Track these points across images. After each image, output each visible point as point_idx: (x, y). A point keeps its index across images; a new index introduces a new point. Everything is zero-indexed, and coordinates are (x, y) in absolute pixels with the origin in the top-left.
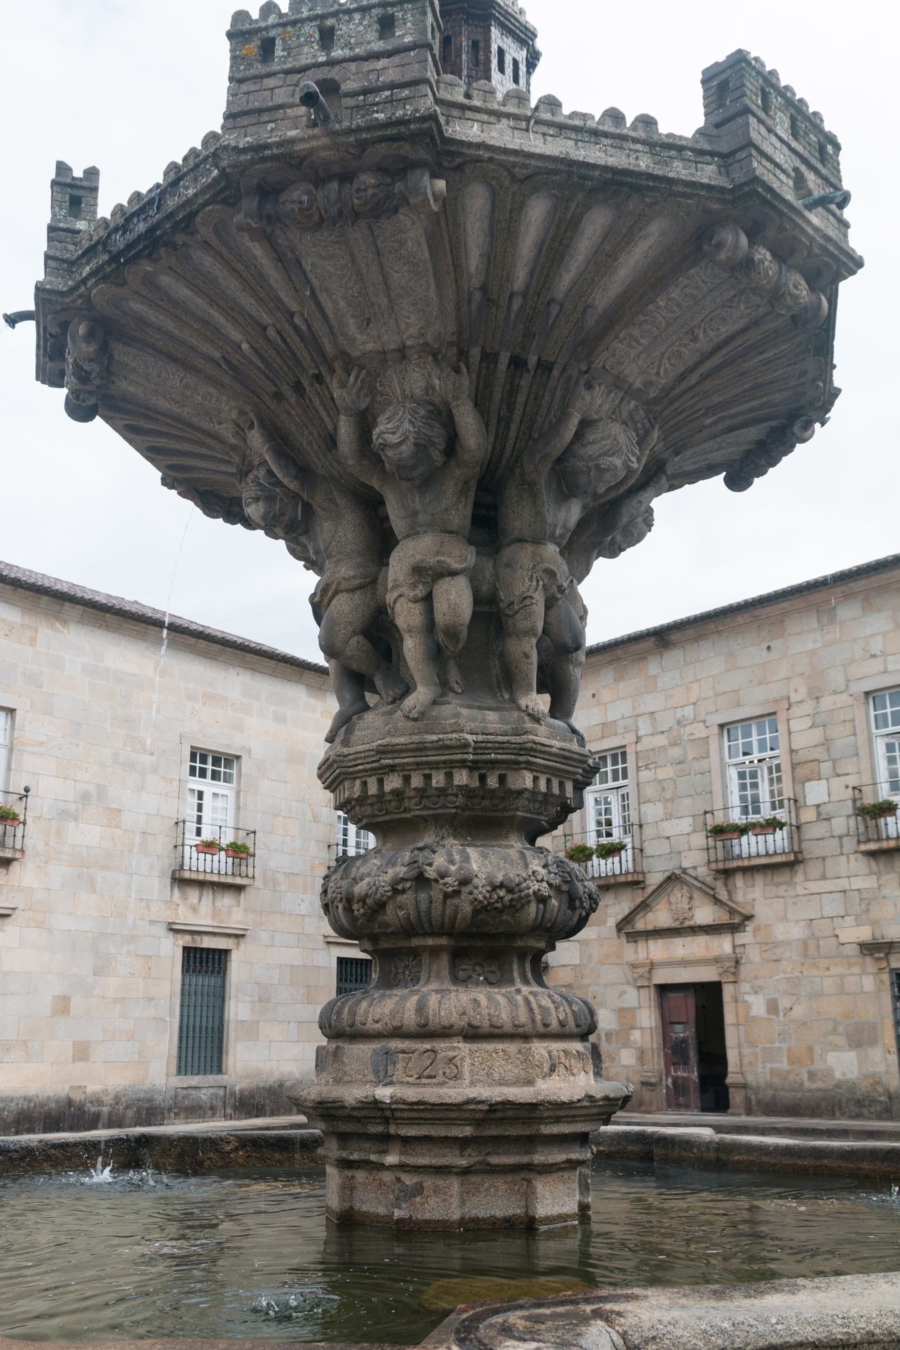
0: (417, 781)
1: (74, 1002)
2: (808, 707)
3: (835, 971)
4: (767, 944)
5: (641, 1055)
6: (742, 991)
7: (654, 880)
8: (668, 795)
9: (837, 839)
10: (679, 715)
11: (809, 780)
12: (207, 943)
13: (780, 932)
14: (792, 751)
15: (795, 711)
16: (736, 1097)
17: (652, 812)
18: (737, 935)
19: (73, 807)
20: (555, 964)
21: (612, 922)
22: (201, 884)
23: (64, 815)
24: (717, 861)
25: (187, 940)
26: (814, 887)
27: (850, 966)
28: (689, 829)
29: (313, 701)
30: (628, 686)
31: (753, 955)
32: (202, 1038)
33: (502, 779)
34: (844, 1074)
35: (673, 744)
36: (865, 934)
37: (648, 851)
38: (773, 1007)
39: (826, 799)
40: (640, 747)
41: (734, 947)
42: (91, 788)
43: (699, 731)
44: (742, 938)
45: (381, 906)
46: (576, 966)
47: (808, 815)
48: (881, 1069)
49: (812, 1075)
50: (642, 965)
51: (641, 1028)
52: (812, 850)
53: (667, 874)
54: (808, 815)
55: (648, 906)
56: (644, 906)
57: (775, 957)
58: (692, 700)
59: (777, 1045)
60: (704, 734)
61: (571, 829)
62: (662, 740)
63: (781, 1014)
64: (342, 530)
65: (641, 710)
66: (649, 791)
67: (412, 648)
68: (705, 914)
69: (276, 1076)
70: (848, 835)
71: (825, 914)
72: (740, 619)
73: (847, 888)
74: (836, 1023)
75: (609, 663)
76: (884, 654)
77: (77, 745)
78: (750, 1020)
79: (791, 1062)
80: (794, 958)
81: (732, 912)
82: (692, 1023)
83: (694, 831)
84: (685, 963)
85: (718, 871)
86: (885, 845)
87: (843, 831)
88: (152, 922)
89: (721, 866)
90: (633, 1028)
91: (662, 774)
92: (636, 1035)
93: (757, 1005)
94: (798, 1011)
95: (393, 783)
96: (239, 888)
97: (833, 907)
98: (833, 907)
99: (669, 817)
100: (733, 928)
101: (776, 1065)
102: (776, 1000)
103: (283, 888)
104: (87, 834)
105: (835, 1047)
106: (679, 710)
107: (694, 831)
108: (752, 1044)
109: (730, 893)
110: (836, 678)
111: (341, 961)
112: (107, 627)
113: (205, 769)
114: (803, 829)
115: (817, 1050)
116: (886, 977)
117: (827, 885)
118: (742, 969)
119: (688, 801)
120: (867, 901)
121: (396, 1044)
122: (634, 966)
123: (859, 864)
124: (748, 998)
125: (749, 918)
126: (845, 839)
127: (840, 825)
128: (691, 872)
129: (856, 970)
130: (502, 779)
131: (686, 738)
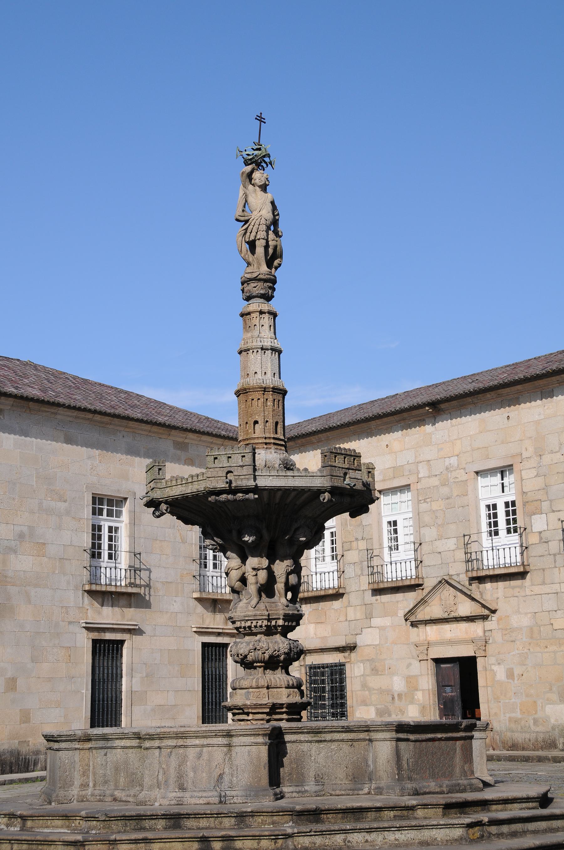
0: (254, 623)
1: (20, 682)
2: (533, 463)
3: (551, 648)
4: (506, 629)
5: (423, 709)
6: (490, 663)
7: (429, 584)
8: (440, 522)
9: (552, 556)
10: (447, 463)
11: (534, 514)
12: (109, 636)
13: (516, 621)
15: (526, 464)
17: (429, 534)
19: (13, 543)
20: (362, 644)
21: (401, 613)
24: (473, 570)
25: (96, 635)
26: (537, 589)
28: (453, 547)
31: (497, 637)
33: (276, 622)
34: (557, 720)
35: (443, 485)
37: (425, 563)
38: (510, 674)
39: (545, 527)
40: (419, 486)
41: (485, 631)
42: (25, 529)
43: (461, 476)
44: (490, 624)
45: (246, 656)
46: (376, 645)
47: (533, 539)
49: (536, 721)
51: (423, 690)
53: (439, 579)
54: (533, 539)
55: (426, 602)
57: (511, 639)
58: (456, 453)
59: (513, 700)
60: (465, 477)
61: (372, 545)
62: (435, 482)
63: (516, 679)
66: (427, 518)
68: (466, 608)
70: (559, 554)
71: (544, 608)
72: (488, 395)
73: (559, 591)
75: (398, 421)
77: (14, 499)
80: (524, 639)
81: (484, 606)
82: (458, 686)
83: (457, 548)
84: (451, 643)
87: (557, 551)
88: (70, 623)
89: (475, 574)
90: (417, 690)
91: (435, 506)
92: (419, 695)
93: (500, 673)
95: (248, 624)
97: (550, 604)
98: (550, 604)
99: (440, 537)
100: (484, 618)
101: (513, 715)
102: (512, 669)
103: (161, 593)
105: (550, 702)
106: (447, 460)
107: (457, 548)
109: (481, 594)
111: (204, 645)
113: (102, 509)
114: (530, 549)
115: (539, 703)
117: (546, 589)
118: (489, 647)
119: (453, 527)
121: (251, 690)
124: (493, 667)
125: (494, 612)
126: (558, 557)
128: (455, 577)
130: (276, 622)
131: (451, 480)
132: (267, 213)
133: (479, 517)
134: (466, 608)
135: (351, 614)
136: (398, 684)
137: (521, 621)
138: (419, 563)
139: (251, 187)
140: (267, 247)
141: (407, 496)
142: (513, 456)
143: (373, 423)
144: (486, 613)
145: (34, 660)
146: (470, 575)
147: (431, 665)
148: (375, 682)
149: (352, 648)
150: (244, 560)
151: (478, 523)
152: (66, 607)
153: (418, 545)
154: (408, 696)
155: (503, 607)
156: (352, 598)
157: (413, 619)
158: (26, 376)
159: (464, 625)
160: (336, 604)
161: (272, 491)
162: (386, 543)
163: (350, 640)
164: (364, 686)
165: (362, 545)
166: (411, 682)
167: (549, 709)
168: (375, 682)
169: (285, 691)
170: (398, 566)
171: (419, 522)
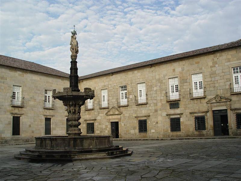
8: (112, 96)
12: (48, 117)
14: (128, 91)
16: (120, 136)
17: (110, 98)
18: (121, 115)
19: (29, 99)
21: (105, 113)
22: (47, 109)
23: (29, 100)
25: (45, 117)
26: (130, 109)
27: (134, 119)
29: (62, 81)
30: (108, 80)
31: (122, 118)
32: (48, 130)
36: (136, 115)
37: (110, 104)
38: (125, 125)
41: (120, 117)
42: (32, 96)
47: (130, 100)
52: (130, 104)
54: (130, 100)
56: (109, 111)
60: (117, 88)
62: (112, 88)
64: (68, 106)
65: (109, 83)
66: (110, 95)
67: (72, 113)
68: (117, 113)
69: (58, 135)
76: (140, 78)
81: (120, 112)
84: (114, 119)
85: (119, 107)
86: (138, 104)
88: (41, 114)
92: (108, 129)
93: (123, 124)
96: (52, 109)
97: (132, 112)
98: (132, 112)
99: (113, 99)
100: (120, 114)
103: (58, 109)
104: (32, 103)
105: (131, 130)
108: (122, 129)
110: (134, 81)
112: (33, 74)
116: (138, 121)
119: (115, 97)
120: (136, 111)
122: (108, 119)
123: (136, 107)
127: (134, 101)
132: (76, 44)
133: (120, 95)
135: (95, 113)
136: (104, 127)
137: (127, 115)
138: (108, 104)
139: (73, 39)
140: (75, 50)
142: (127, 84)
145: (34, 122)
147: (110, 123)
148: (100, 126)
149: (95, 120)
150: (70, 107)
151: (120, 96)
153: (108, 100)
154: (106, 129)
155: (124, 113)
156: (96, 110)
157: (107, 114)
158: (32, 65)
159: (116, 116)
160: (93, 111)
161: (75, 96)
162: (102, 100)
163: (95, 118)
164: (97, 127)
165: (98, 100)
166: (106, 126)
167: (131, 131)
168: (100, 126)
169: (77, 131)
170: (105, 104)
171: (109, 96)
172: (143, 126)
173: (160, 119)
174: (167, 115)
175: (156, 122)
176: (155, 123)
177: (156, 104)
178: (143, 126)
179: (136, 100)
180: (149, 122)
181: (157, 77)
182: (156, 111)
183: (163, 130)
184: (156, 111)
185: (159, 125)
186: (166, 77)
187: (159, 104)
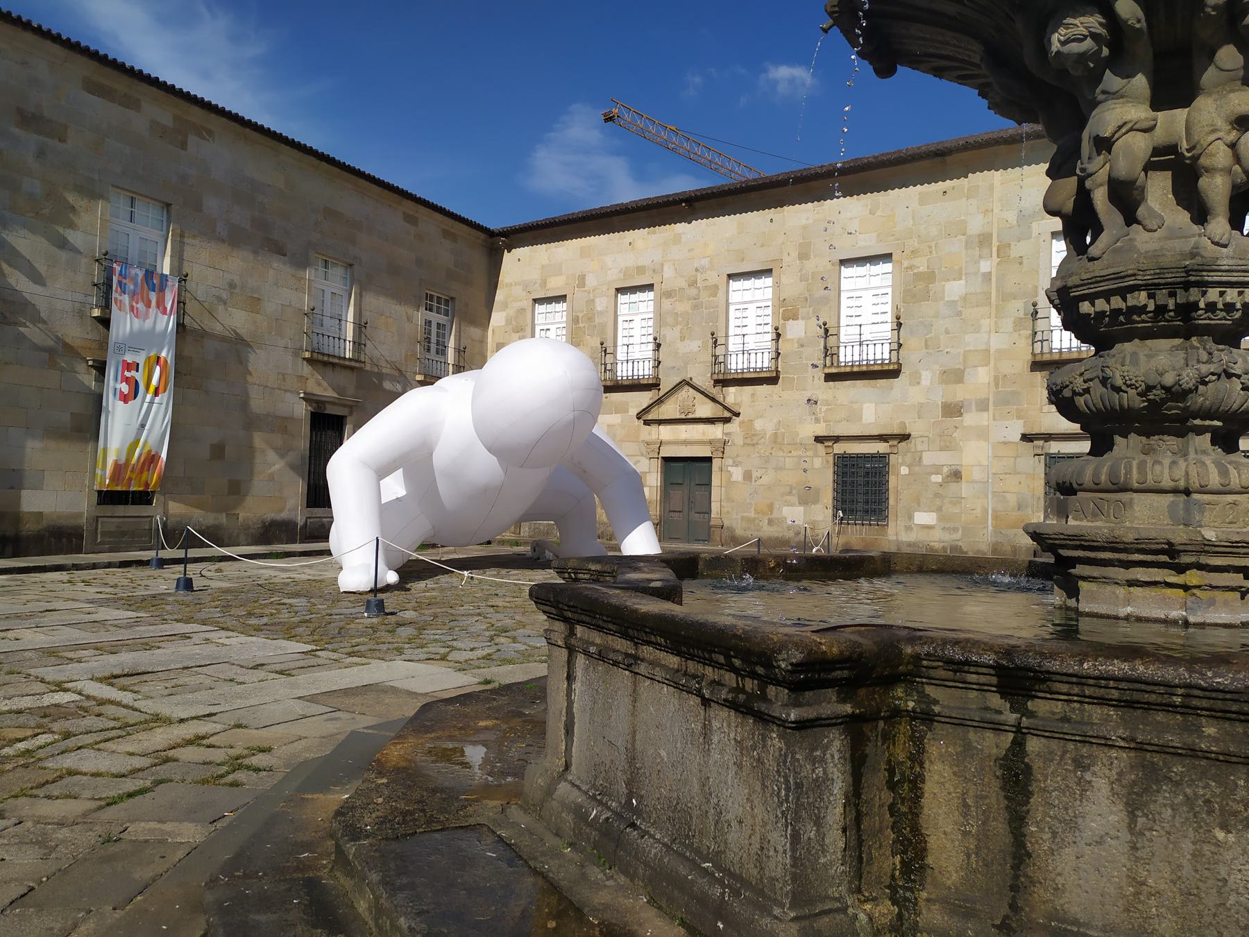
12: (330, 410)
16: (716, 535)
21: (634, 412)
36: (822, 432)
38: (748, 476)
48: (820, 518)
49: (770, 522)
50: (655, 443)
56: (659, 401)
68: (705, 409)
74: (791, 488)
78: (731, 484)
79: (757, 512)
81: (726, 408)
84: (686, 443)
89: (721, 377)
94: (766, 480)
100: (726, 420)
108: (729, 500)
116: (831, 459)
125: (738, 415)
129: (810, 453)
134: (705, 409)
141: (651, 295)
143: (615, 219)
144: (728, 416)
146: (715, 377)
152: (283, 375)
172: (861, 483)
173: (975, 456)
174: (1026, 438)
175: (945, 470)
176: (937, 479)
177: (954, 376)
178: (861, 483)
179: (830, 353)
180: (904, 470)
181: (976, 225)
182: (953, 410)
183: (995, 517)
184: (953, 410)
185: (965, 489)
186: (1034, 225)
187: (982, 376)
